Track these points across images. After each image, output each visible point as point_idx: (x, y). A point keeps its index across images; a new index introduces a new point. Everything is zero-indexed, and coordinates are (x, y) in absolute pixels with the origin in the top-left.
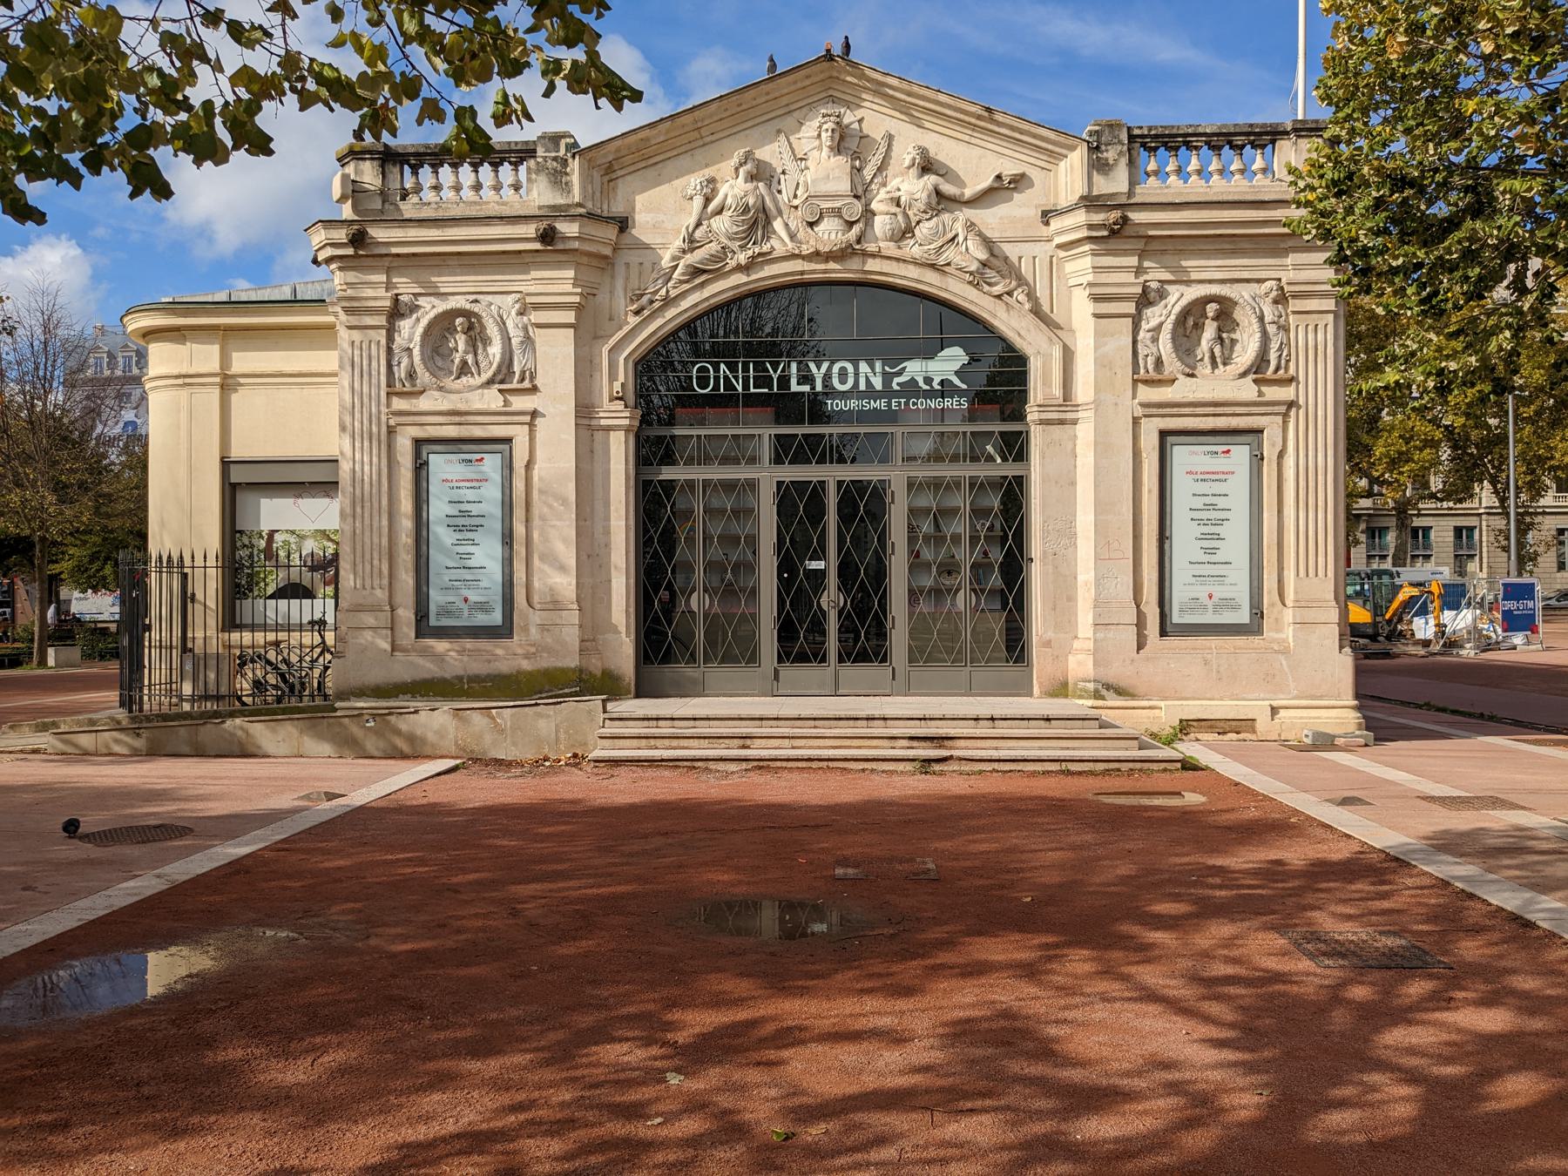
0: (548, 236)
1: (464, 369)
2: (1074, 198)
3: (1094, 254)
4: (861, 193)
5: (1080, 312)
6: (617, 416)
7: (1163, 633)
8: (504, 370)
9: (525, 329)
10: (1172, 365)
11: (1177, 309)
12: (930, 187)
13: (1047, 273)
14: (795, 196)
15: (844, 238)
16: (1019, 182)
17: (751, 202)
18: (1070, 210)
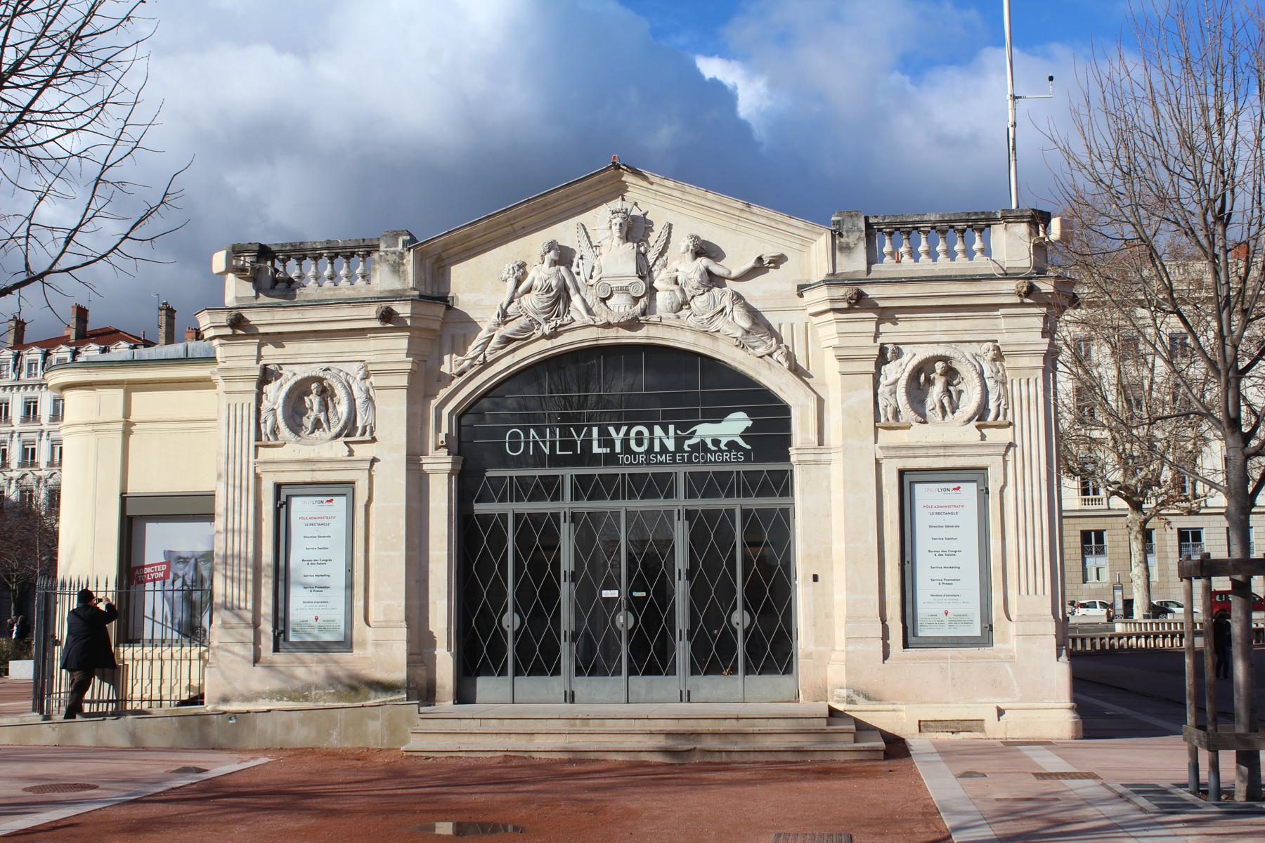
0: (388, 316)
1: (317, 425)
2: (822, 276)
3: (838, 321)
4: (644, 272)
5: (827, 370)
6: (439, 464)
7: (906, 645)
8: (350, 426)
9: (367, 391)
10: (907, 414)
11: (910, 368)
12: (702, 268)
13: (803, 336)
14: (591, 277)
15: (631, 312)
16: (778, 261)
17: (554, 284)
18: (817, 285)
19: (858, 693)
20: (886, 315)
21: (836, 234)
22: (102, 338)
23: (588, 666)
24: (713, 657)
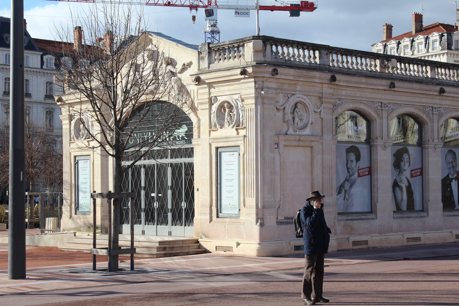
7: (218, 217)
19: (203, 234)
20: (210, 85)
21: (200, 53)
22: (428, 31)
24: (177, 220)
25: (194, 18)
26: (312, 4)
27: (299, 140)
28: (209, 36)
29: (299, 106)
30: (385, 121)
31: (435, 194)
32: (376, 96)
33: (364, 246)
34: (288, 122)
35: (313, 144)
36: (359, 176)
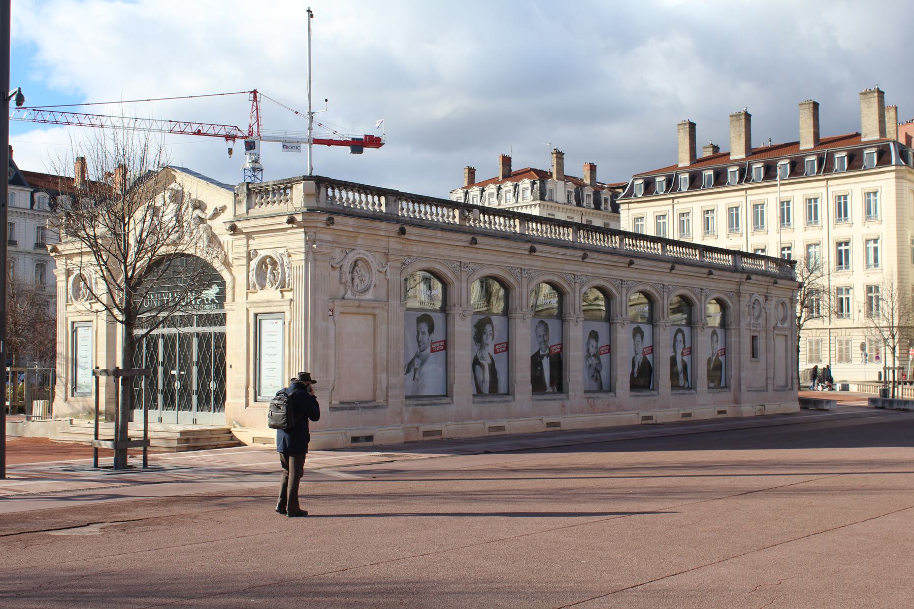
7: (256, 401)
19: (237, 423)
20: (249, 236)
21: (236, 195)
23: (200, 407)
24: (204, 403)
25: (230, 151)
26: (378, 139)
27: (359, 306)
28: (249, 174)
29: (360, 264)
30: (464, 285)
31: (523, 373)
32: (454, 254)
33: (437, 437)
34: (345, 284)
35: (377, 311)
36: (432, 351)
